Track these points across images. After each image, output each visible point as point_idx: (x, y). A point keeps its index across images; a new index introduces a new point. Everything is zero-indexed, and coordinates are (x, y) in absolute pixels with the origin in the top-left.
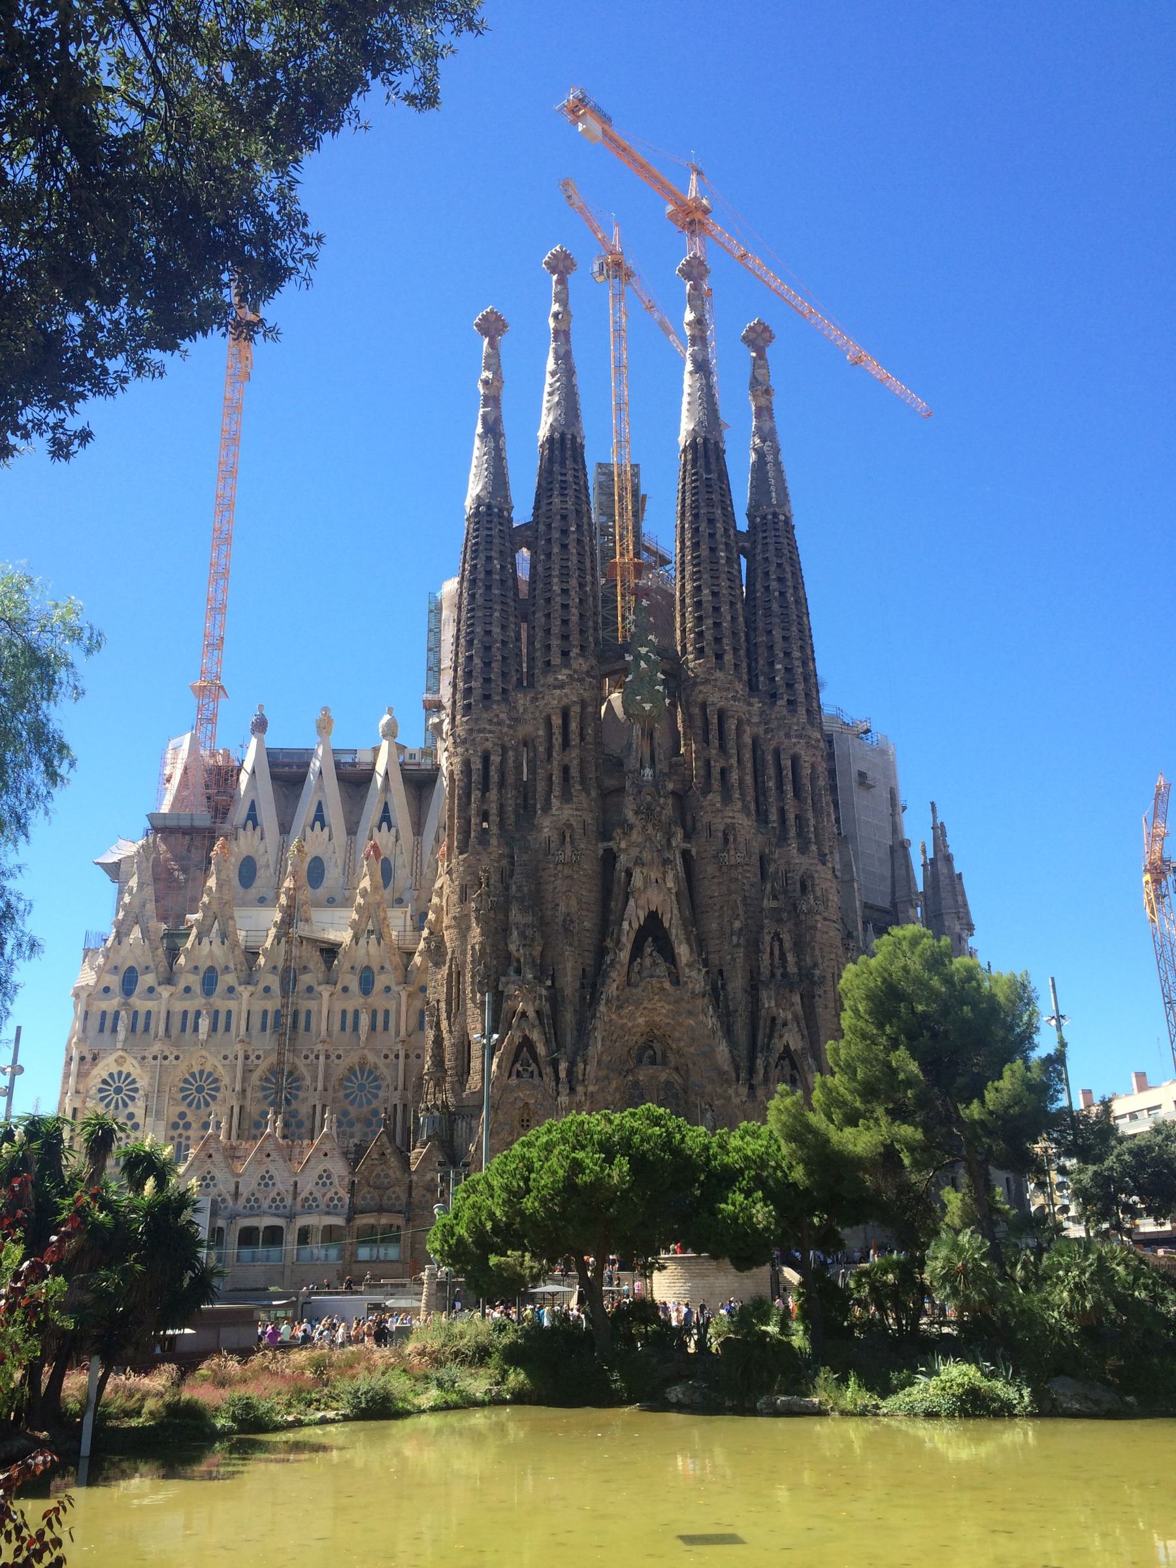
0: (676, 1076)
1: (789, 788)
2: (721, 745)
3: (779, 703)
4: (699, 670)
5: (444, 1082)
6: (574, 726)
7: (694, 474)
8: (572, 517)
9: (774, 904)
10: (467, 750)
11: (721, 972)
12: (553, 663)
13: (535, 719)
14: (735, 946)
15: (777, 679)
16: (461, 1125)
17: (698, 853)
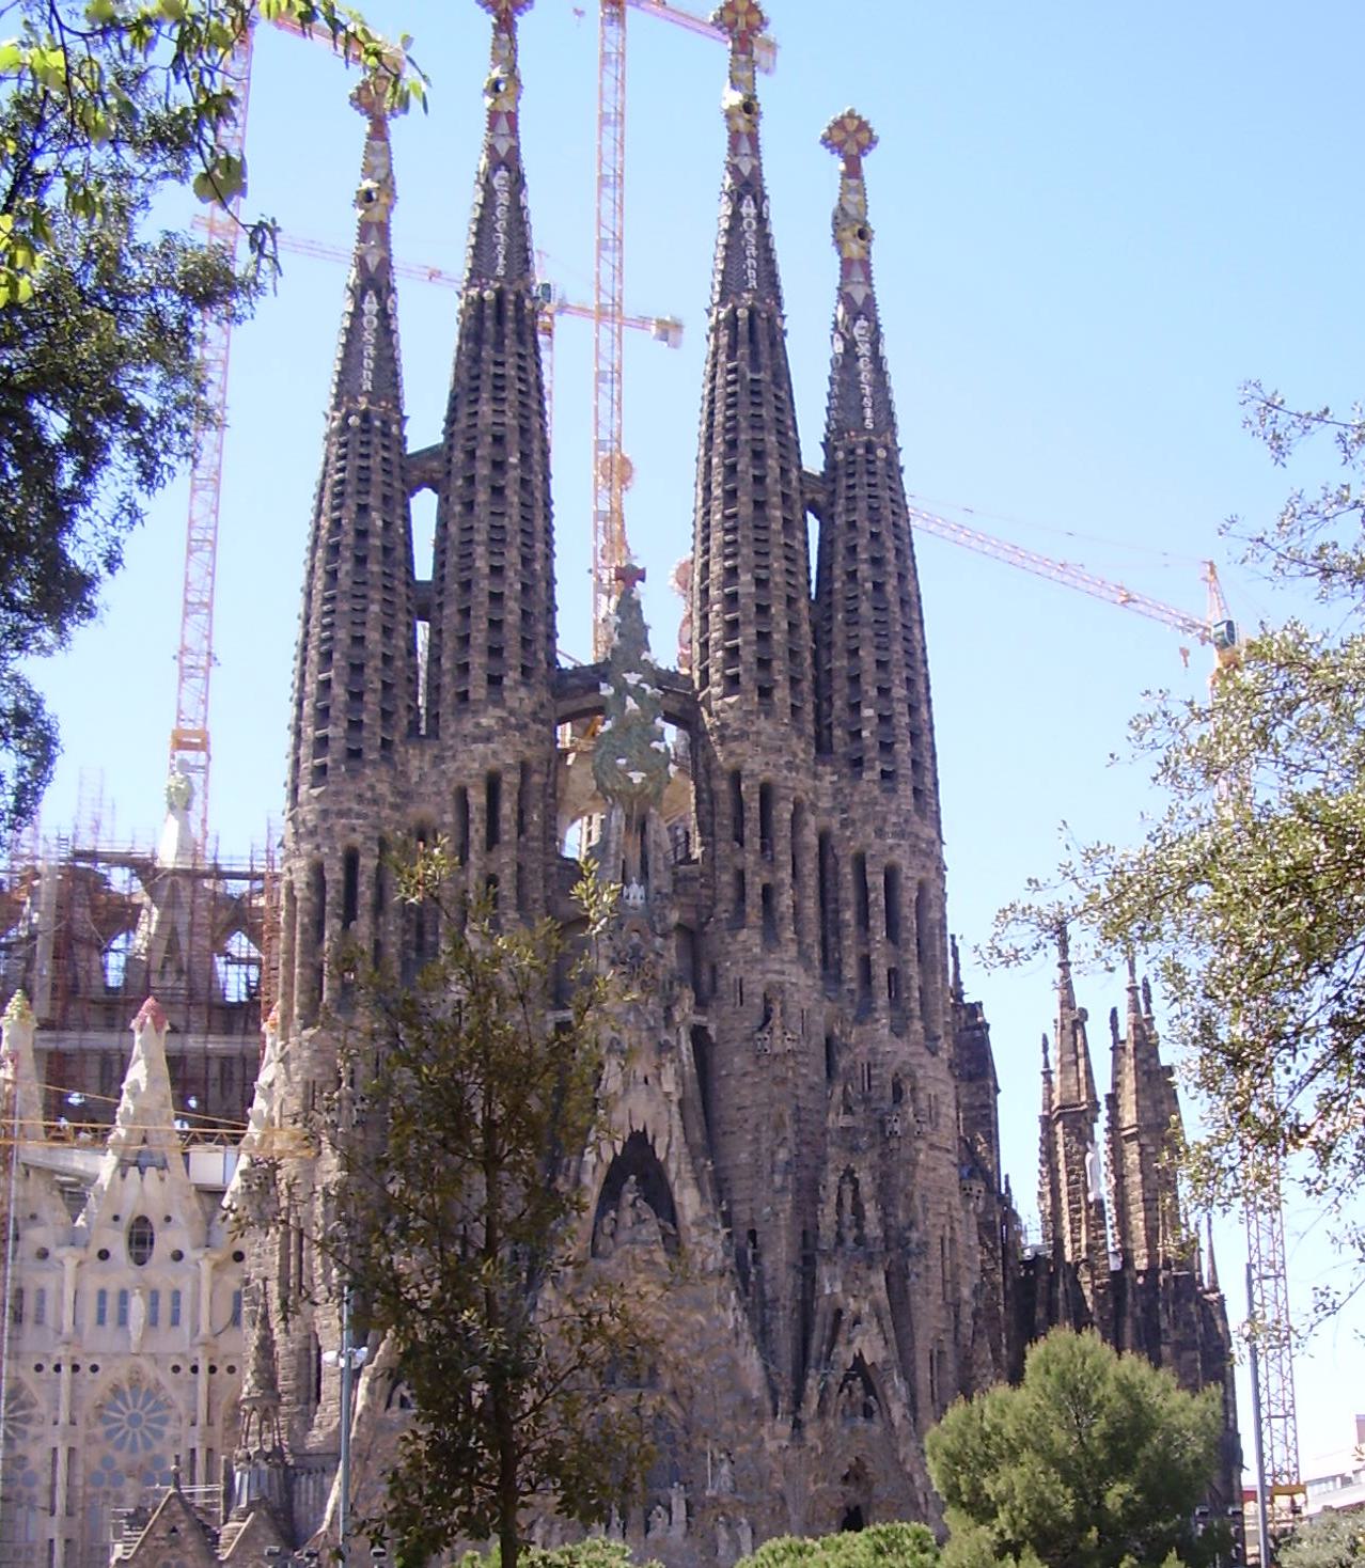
0: (672, 1406)
1: (878, 923)
2: (764, 847)
3: (866, 776)
4: (729, 716)
5: (277, 1413)
6: (507, 808)
7: (730, 372)
8: (513, 439)
9: (844, 1121)
10: (318, 847)
11: (752, 1234)
12: (472, 696)
13: (439, 793)
14: (776, 1192)
15: (865, 734)
16: (306, 1484)
17: (720, 1031)
